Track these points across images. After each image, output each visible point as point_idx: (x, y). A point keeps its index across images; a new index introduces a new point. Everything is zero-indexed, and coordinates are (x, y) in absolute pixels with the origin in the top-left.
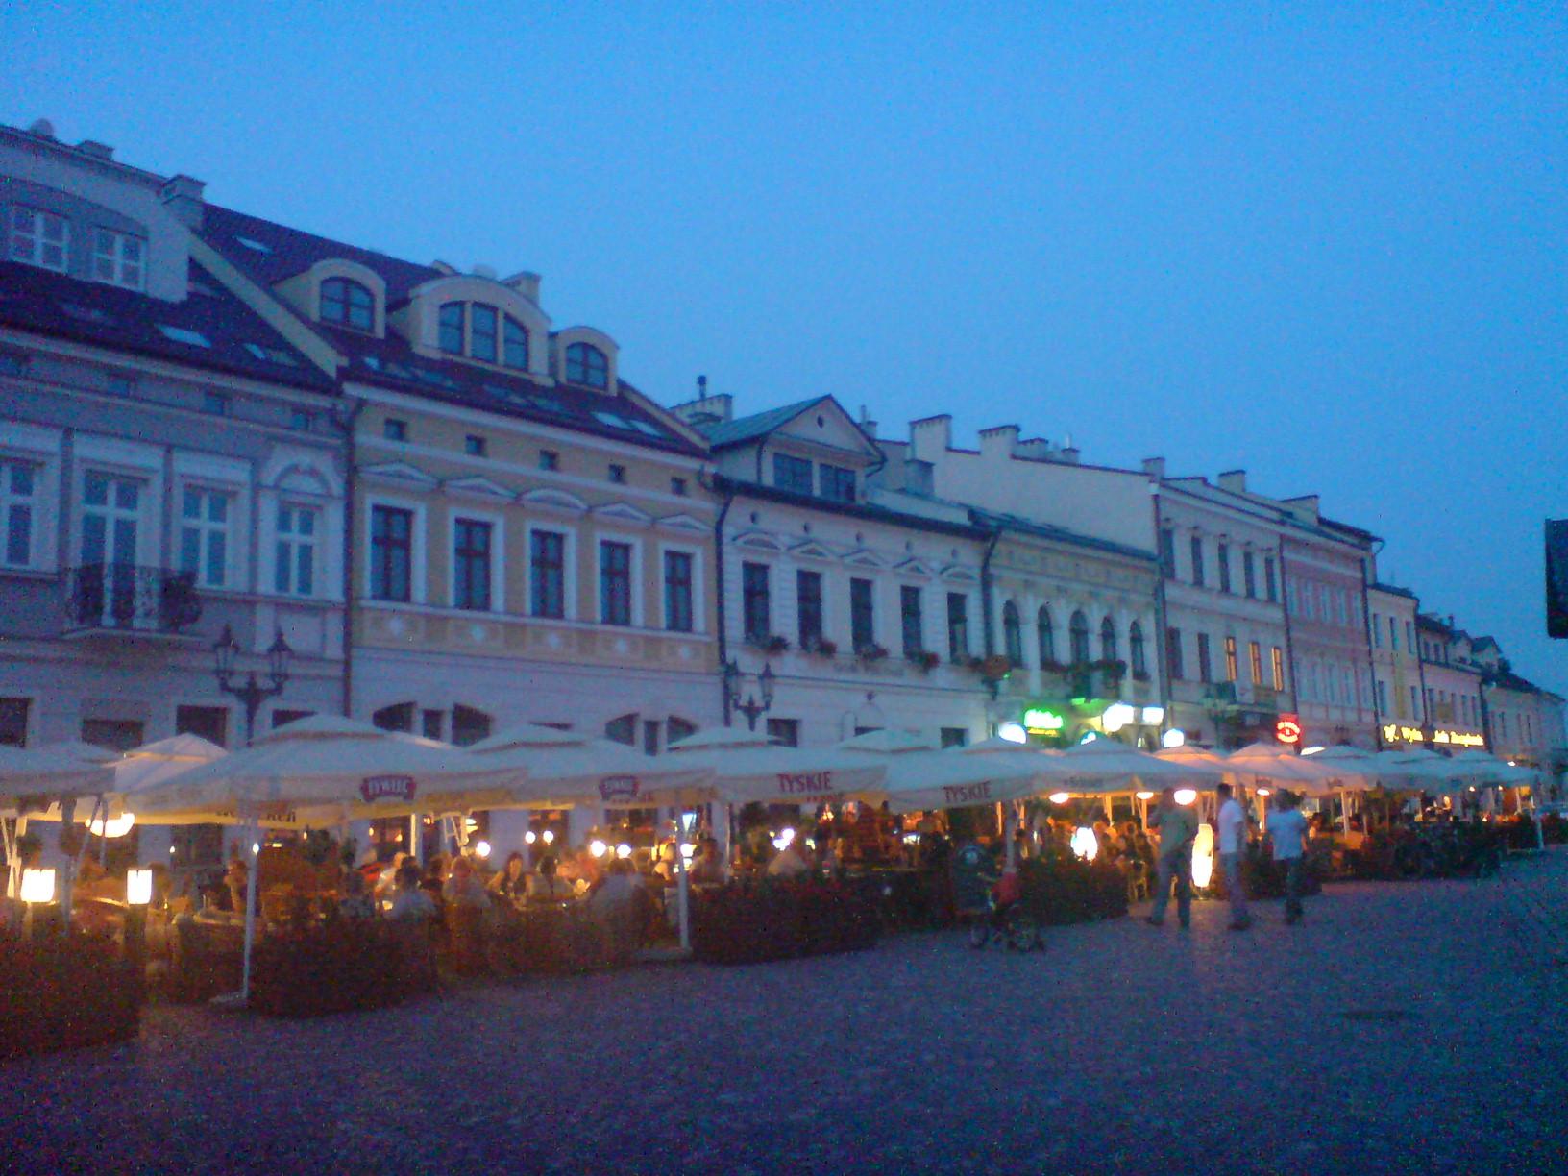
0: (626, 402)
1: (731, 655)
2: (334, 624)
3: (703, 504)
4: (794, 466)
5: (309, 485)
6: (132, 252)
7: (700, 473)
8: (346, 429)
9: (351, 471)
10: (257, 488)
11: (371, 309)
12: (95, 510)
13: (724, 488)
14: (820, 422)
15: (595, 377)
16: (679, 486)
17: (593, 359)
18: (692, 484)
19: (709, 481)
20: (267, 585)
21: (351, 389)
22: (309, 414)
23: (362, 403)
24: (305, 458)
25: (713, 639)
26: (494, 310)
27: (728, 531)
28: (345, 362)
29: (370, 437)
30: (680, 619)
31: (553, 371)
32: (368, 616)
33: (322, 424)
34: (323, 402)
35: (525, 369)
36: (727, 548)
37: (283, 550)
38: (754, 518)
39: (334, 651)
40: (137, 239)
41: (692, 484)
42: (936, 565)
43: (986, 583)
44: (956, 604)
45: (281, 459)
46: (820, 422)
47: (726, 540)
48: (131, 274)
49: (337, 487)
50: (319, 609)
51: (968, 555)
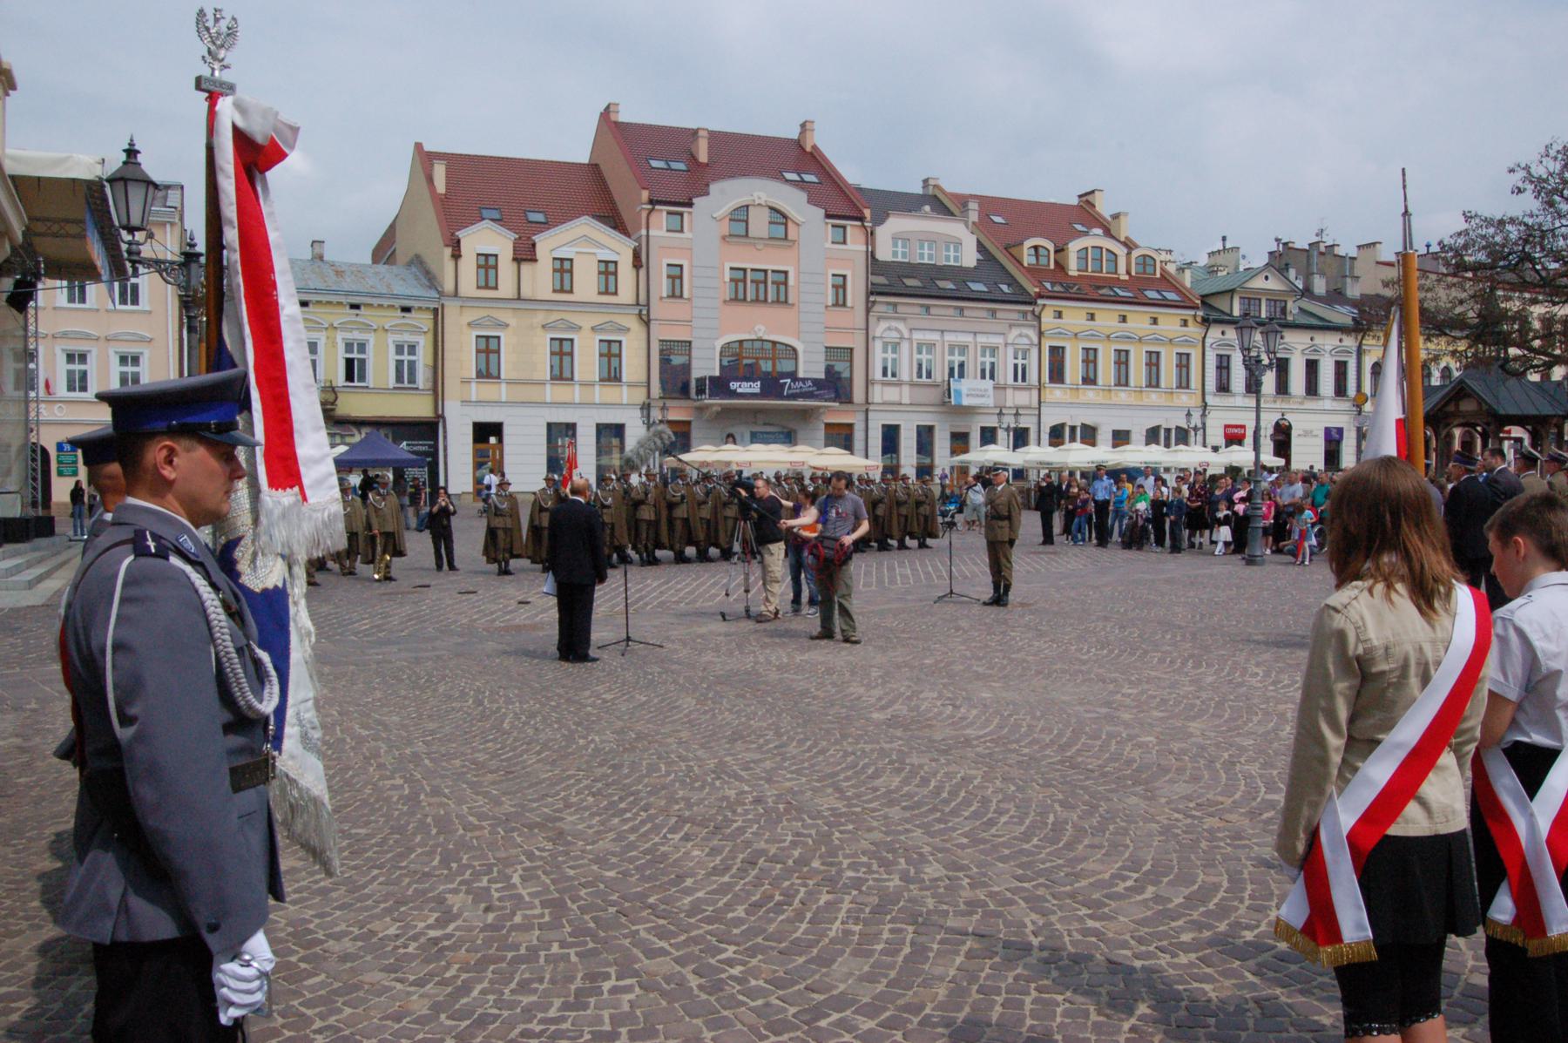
0: (1166, 281)
1: (1210, 400)
2: (1035, 393)
3: (1194, 330)
4: (1251, 300)
5: (1025, 341)
6: (956, 251)
7: (1195, 316)
8: (1039, 318)
9: (1041, 334)
10: (1006, 345)
11: (1049, 256)
12: (952, 358)
13: (1206, 322)
14: (1267, 278)
15: (1149, 270)
16: (1185, 323)
17: (1149, 261)
18: (1190, 322)
19: (1199, 319)
20: (1010, 380)
21: (1040, 302)
22: (1025, 313)
23: (1044, 305)
24: (1025, 331)
25: (1199, 392)
26: (1101, 248)
27: (1209, 341)
28: (1037, 290)
29: (1048, 318)
30: (1184, 383)
31: (1128, 273)
32: (1048, 391)
33: (1030, 317)
34: (1030, 308)
35: (1116, 273)
36: (1207, 349)
37: (1016, 366)
38: (1223, 333)
39: (1035, 403)
40: (958, 244)
41: (1190, 322)
42: (1328, 348)
43: (1360, 352)
44: (1341, 368)
45: (1015, 332)
46: (1267, 278)
47: (1207, 345)
48: (956, 259)
49: (1035, 340)
50: (1029, 388)
51: (1350, 342)
